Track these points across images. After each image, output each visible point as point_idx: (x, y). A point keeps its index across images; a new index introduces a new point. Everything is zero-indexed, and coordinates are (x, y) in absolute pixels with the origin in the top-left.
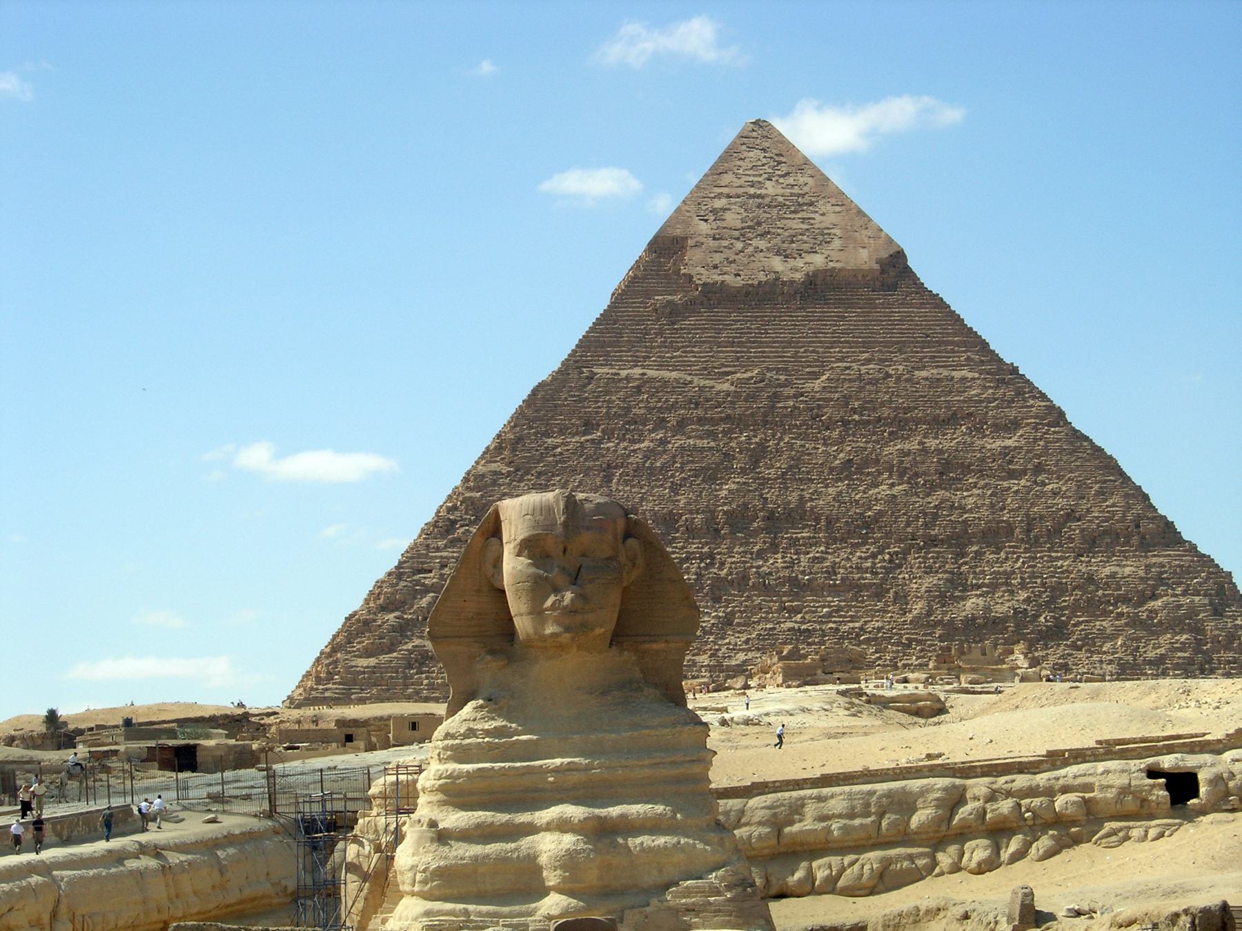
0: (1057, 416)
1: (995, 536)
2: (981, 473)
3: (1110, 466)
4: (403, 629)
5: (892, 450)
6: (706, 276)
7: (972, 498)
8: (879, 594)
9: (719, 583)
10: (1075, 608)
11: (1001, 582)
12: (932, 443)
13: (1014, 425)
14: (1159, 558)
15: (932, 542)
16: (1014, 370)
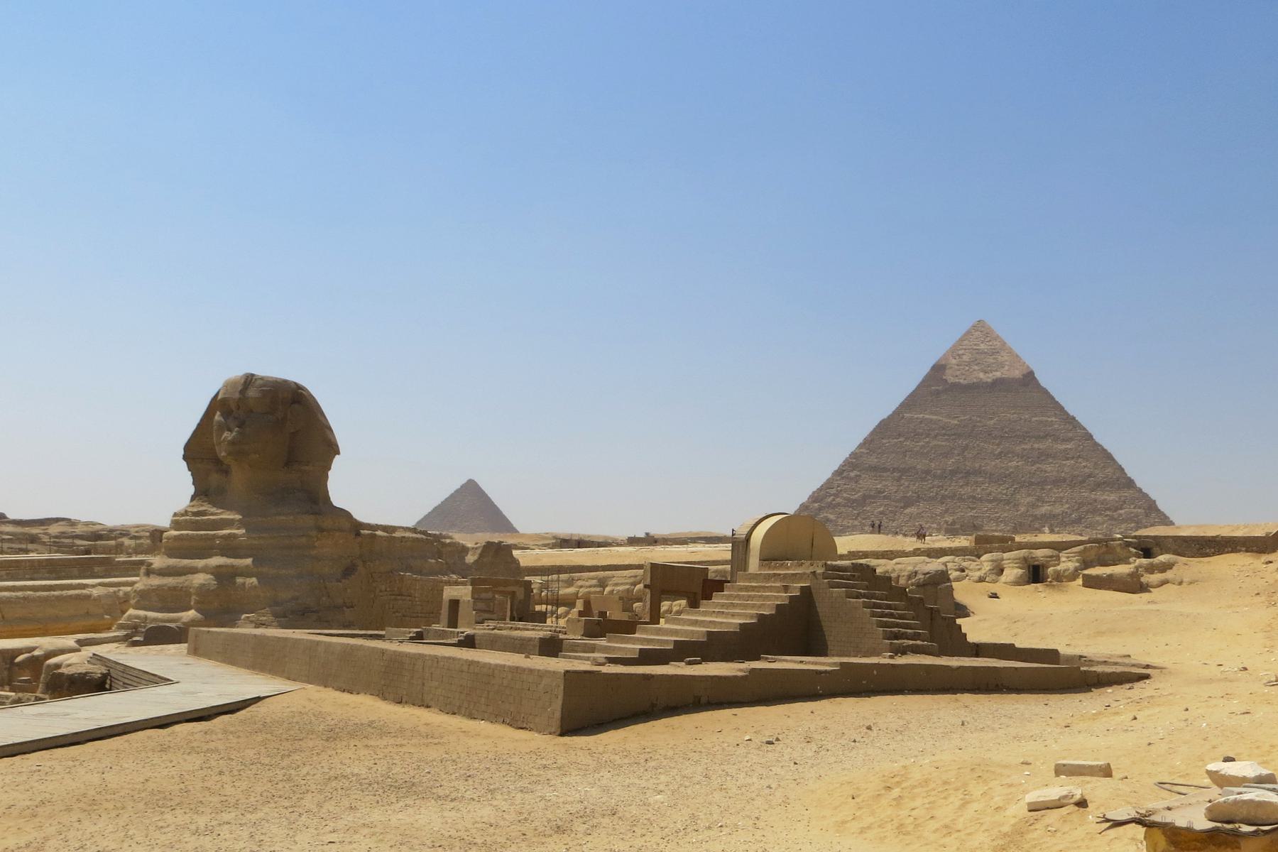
0: (1090, 437)
1: (1057, 482)
2: (1054, 458)
3: (1109, 457)
4: (820, 509)
5: (1018, 449)
6: (951, 380)
7: (1049, 468)
8: (1008, 502)
9: (944, 497)
10: (1087, 512)
11: (1059, 501)
12: (1036, 446)
13: (1071, 439)
14: (1127, 493)
15: (1031, 484)
16: (1074, 418)
